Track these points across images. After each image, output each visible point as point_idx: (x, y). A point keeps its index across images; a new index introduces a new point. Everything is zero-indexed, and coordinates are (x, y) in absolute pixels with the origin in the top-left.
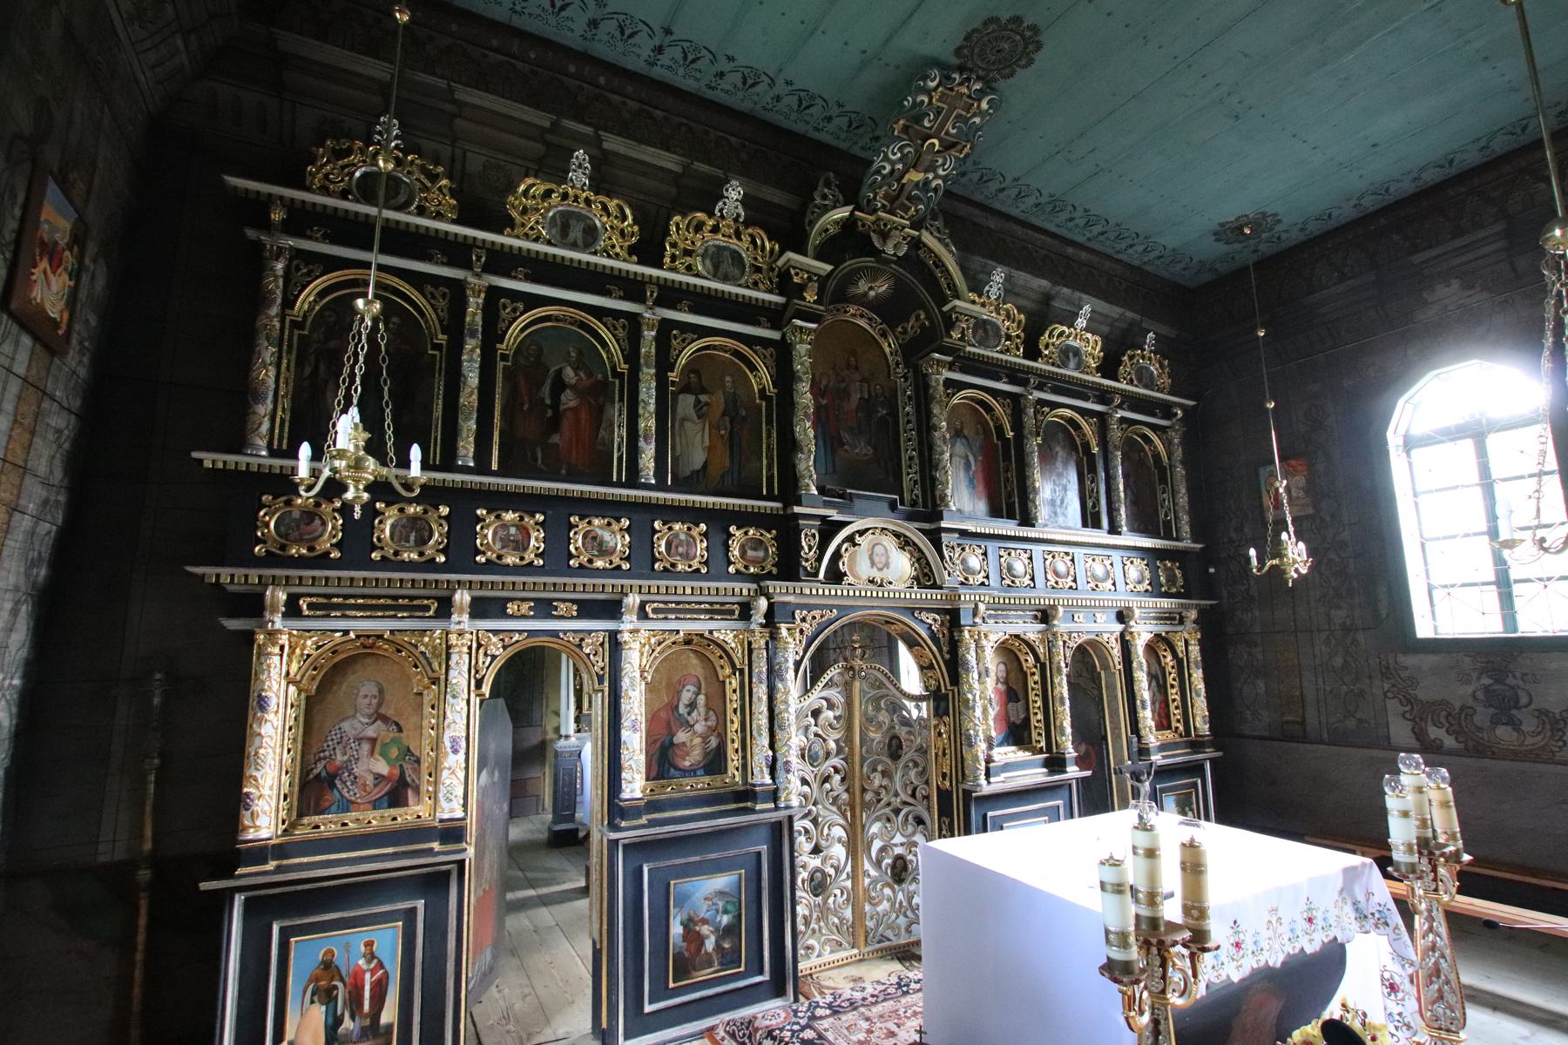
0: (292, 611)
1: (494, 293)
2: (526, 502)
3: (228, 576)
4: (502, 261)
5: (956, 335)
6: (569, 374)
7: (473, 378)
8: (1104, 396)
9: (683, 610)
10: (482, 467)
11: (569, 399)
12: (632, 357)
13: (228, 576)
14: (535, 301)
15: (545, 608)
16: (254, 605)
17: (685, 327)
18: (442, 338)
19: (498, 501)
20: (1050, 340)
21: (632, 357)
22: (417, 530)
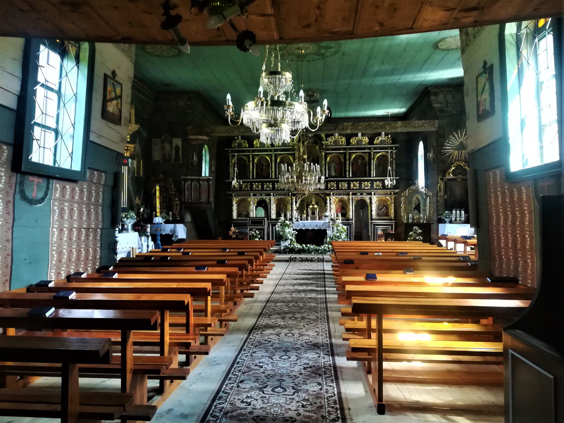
0: (235, 196)
1: (253, 155)
2: (258, 182)
3: (229, 193)
4: (254, 151)
5: (324, 147)
6: (264, 163)
7: (251, 167)
8: (370, 149)
9: (280, 195)
10: (253, 178)
11: (264, 167)
12: (271, 160)
13: (229, 193)
14: (258, 155)
15: (261, 195)
16: (231, 195)
17: (279, 154)
18: (247, 162)
19: (255, 182)
20: (353, 141)
21: (271, 160)
22: (246, 186)
